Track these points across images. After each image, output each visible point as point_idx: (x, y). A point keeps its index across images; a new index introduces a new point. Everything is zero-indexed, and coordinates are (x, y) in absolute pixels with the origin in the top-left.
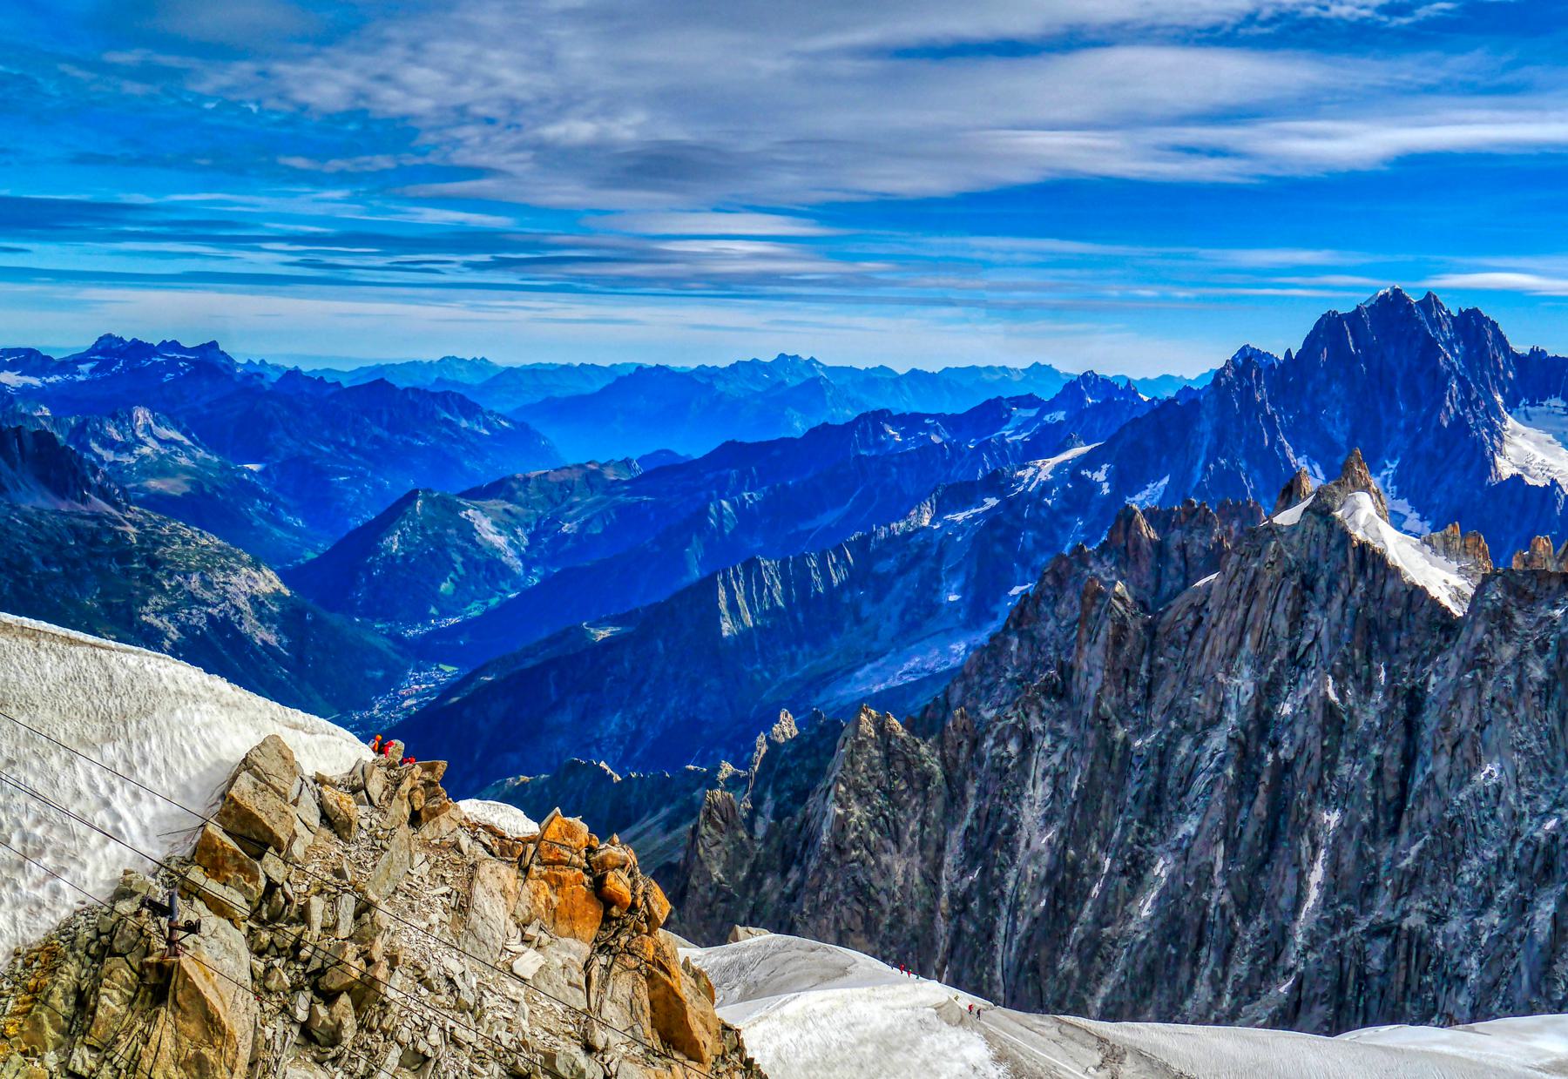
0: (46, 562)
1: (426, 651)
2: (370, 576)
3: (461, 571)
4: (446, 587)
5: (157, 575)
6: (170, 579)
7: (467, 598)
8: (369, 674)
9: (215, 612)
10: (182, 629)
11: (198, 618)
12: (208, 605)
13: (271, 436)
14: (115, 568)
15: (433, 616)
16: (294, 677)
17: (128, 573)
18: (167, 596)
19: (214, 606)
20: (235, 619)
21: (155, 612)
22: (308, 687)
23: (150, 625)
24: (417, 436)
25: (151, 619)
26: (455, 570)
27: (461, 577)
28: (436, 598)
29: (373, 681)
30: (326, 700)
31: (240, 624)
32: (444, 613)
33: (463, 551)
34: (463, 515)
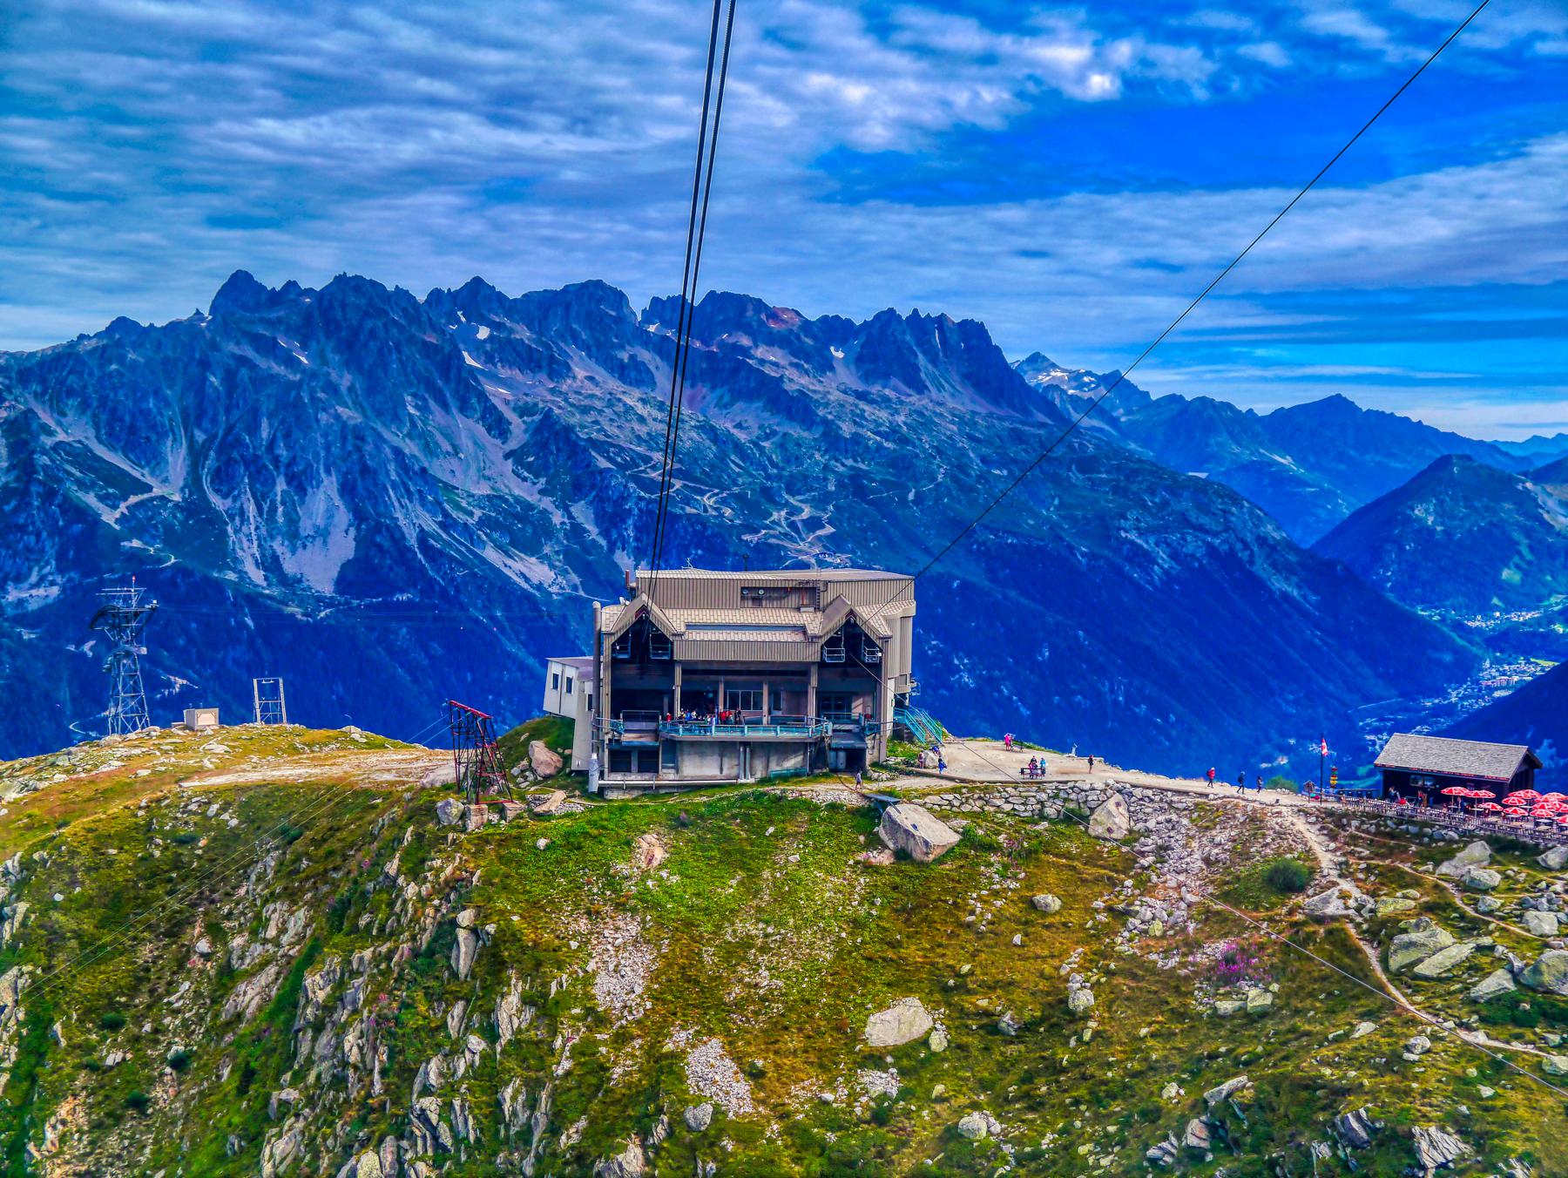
0: (984, 460)
1: (1508, 643)
2: (1402, 550)
3: (1529, 556)
4: (1509, 575)
5: (1134, 487)
6: (1153, 493)
7: (1544, 591)
8: (1435, 655)
9: (1217, 542)
10: (1174, 556)
11: (1193, 546)
12: (1207, 532)
13: (1212, 441)
14: (1076, 477)
15: (1497, 608)
16: (1330, 641)
17: (1094, 485)
18: (1152, 515)
19: (1215, 535)
20: (1244, 555)
21: (1137, 529)
22: (1352, 657)
23: (1133, 543)
24: (1391, 455)
25: (1133, 536)
26: (1520, 554)
27: (1530, 563)
28: (1501, 588)
29: (1439, 663)
30: (1380, 676)
31: (1252, 562)
32: (1511, 606)
33: (1528, 532)
34: (1520, 487)
